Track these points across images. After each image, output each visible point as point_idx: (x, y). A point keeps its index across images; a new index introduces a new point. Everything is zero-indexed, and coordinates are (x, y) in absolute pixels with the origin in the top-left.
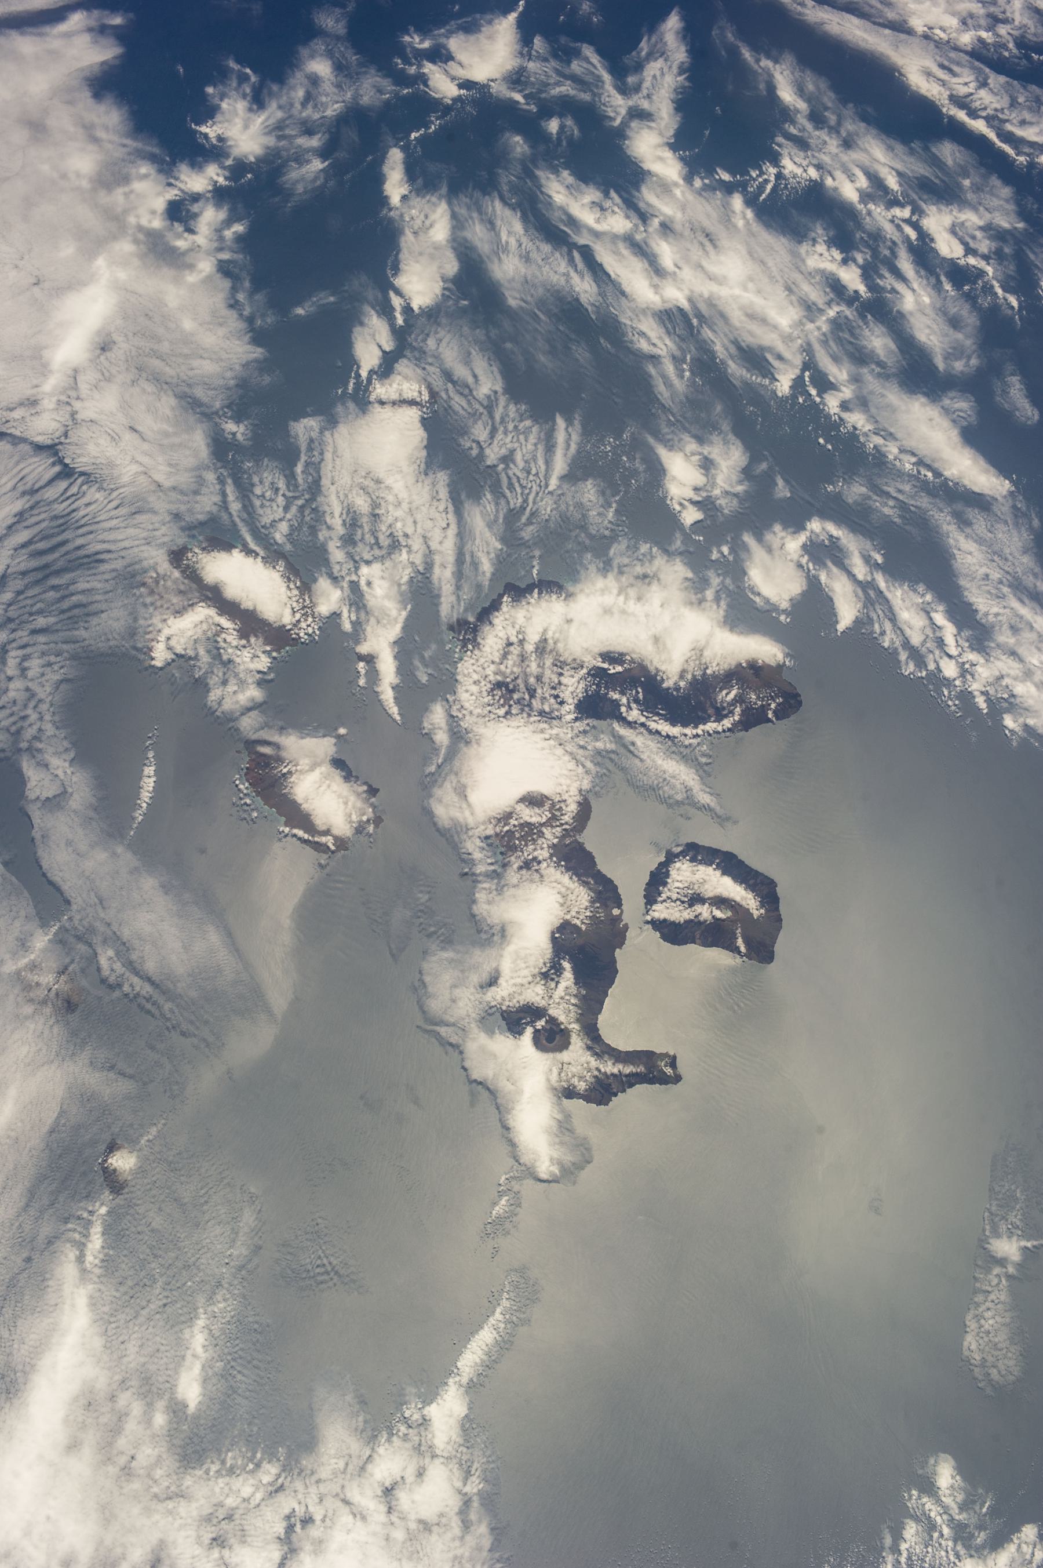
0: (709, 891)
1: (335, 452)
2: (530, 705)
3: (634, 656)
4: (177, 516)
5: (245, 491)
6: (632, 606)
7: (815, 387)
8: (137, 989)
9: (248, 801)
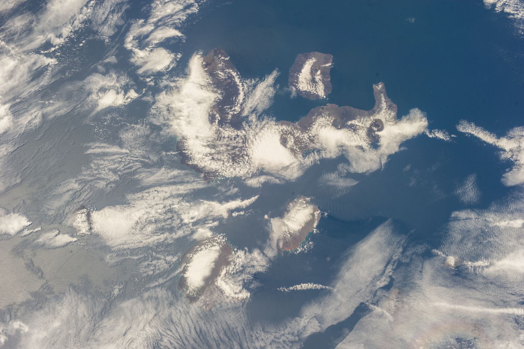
0: (309, 77)
1: (123, 244)
2: (241, 147)
3: (209, 111)
4: (171, 304)
5: (151, 278)
6: (185, 113)
8: (390, 270)
9: (305, 246)
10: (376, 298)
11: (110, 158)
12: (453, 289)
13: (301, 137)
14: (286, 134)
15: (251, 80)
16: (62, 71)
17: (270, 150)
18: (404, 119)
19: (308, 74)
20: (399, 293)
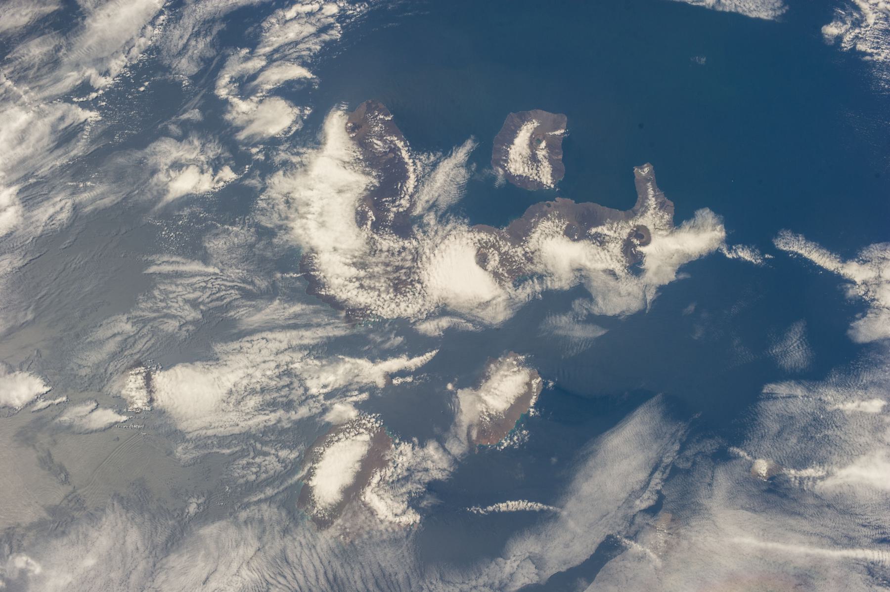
0: (526, 152)
1: (206, 428)
2: (409, 268)
3: (357, 205)
4: (285, 531)
6: (316, 208)
7: (89, 94)
8: (658, 481)
9: (515, 438)
10: (633, 528)
11: (187, 282)
12: (764, 515)
13: (511, 252)
14: (486, 248)
15: (429, 155)
16: (108, 133)
17: (459, 273)
18: (686, 225)
19: (525, 146)
20: (673, 520)
